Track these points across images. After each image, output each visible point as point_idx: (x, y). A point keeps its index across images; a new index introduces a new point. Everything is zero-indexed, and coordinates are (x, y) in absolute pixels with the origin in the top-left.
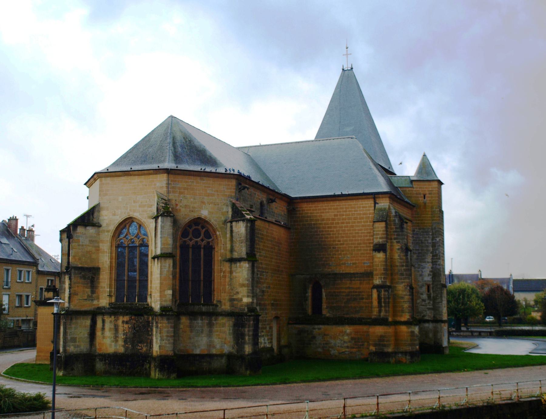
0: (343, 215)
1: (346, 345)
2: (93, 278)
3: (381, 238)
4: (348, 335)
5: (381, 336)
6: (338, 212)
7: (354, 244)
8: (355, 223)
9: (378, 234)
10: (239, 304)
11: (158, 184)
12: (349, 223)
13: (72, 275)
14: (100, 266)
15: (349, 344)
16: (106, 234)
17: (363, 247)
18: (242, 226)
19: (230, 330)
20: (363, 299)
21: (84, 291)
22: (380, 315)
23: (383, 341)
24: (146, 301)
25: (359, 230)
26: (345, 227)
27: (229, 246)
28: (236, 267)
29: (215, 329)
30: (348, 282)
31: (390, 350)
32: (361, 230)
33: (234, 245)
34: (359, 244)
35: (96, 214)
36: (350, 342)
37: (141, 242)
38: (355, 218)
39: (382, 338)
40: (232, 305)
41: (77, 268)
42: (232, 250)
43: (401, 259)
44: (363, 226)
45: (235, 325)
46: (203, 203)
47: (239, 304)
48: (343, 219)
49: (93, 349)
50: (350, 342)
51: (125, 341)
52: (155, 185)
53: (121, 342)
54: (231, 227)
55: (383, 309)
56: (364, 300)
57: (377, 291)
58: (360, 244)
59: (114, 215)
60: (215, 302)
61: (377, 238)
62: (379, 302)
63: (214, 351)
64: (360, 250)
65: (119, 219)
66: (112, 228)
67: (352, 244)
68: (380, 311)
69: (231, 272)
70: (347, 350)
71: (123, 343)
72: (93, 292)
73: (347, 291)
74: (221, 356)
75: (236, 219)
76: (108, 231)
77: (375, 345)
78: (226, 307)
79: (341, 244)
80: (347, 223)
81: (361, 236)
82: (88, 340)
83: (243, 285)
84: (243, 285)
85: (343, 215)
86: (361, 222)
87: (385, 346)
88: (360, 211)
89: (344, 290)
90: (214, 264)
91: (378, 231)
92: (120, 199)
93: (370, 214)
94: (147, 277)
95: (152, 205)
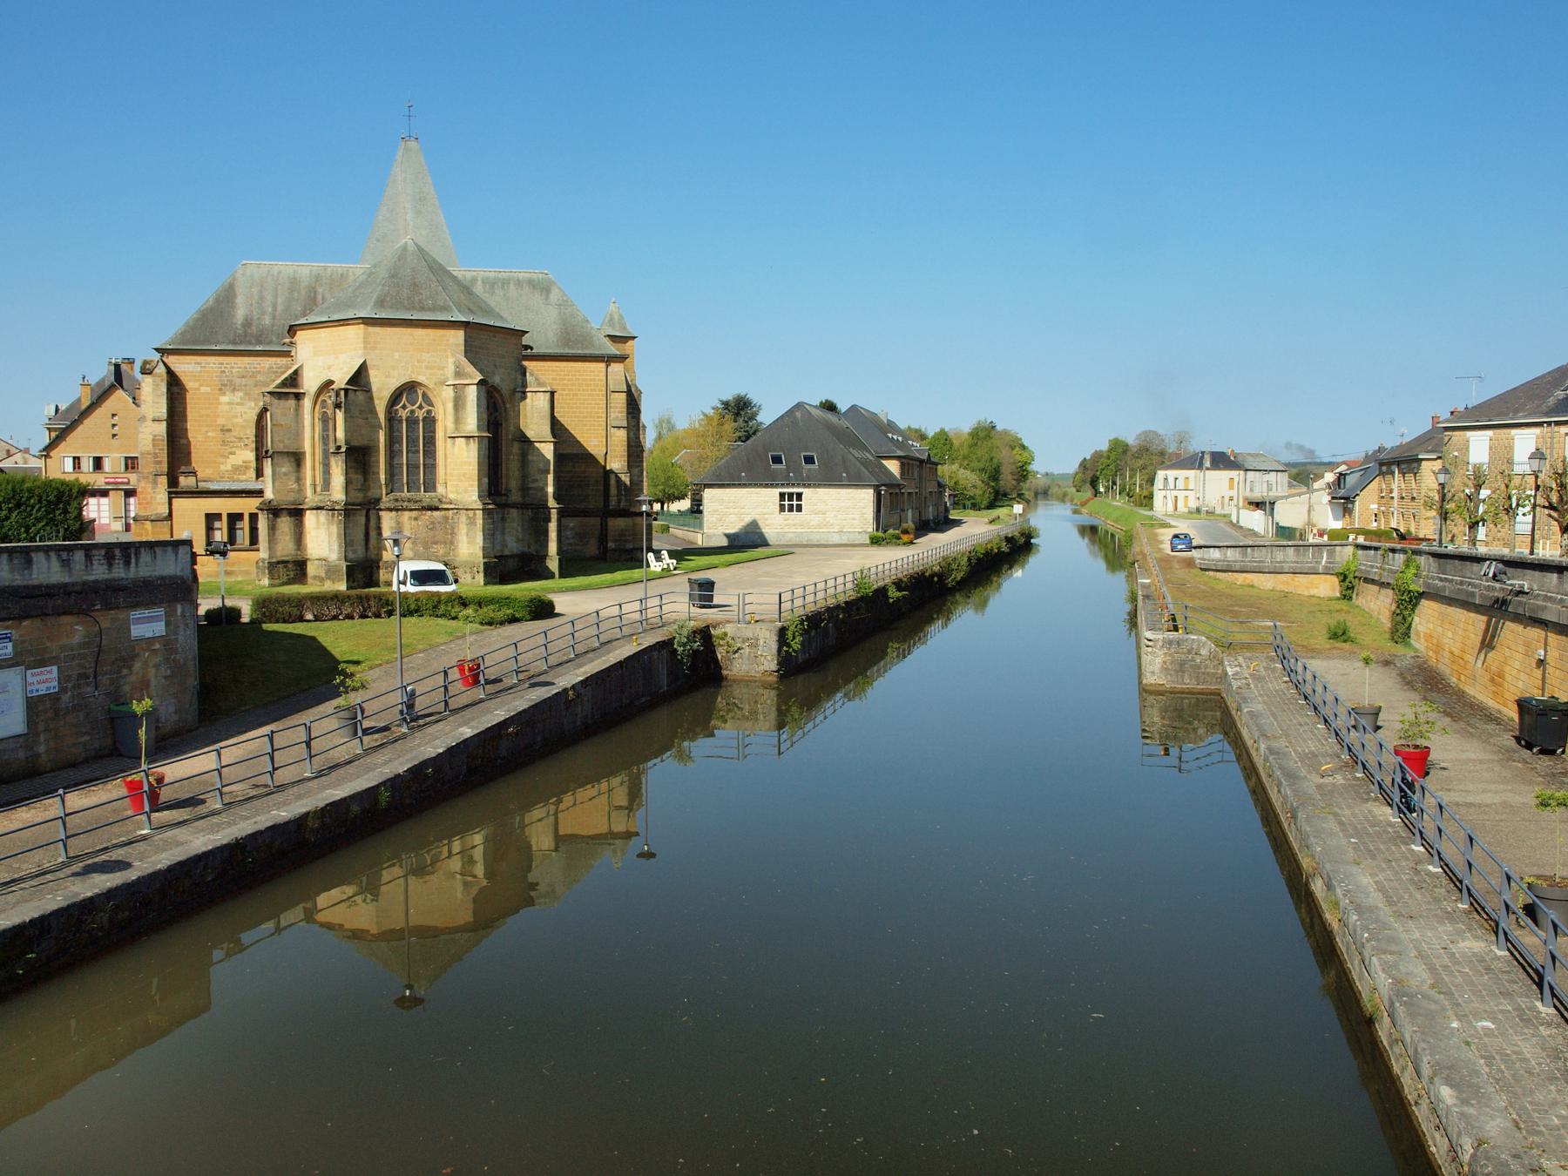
0: (564, 380)
1: (568, 541)
3: (619, 412)
4: (571, 529)
5: (622, 530)
6: (557, 375)
7: (578, 417)
8: (579, 390)
9: (617, 407)
10: (539, 494)
12: (572, 390)
15: (572, 541)
17: (589, 421)
18: (542, 398)
23: (625, 536)
24: (435, 491)
25: (584, 400)
26: (567, 395)
29: (507, 525)
31: (631, 547)
32: (587, 400)
34: (584, 417)
35: (363, 373)
36: (573, 538)
38: (580, 385)
40: (524, 496)
44: (589, 395)
45: (532, 519)
46: (495, 366)
47: (539, 494)
48: (564, 385)
49: (369, 554)
50: (573, 538)
59: (388, 376)
60: (503, 492)
61: (614, 412)
63: (507, 552)
64: (586, 425)
65: (395, 383)
67: (575, 417)
68: (619, 501)
72: (365, 480)
74: (513, 556)
77: (615, 541)
78: (515, 497)
80: (569, 390)
81: (587, 408)
82: (363, 543)
85: (564, 380)
86: (587, 390)
87: (626, 541)
88: (587, 375)
91: (617, 403)
92: (397, 355)
93: (599, 380)
94: (435, 460)
95: (444, 367)
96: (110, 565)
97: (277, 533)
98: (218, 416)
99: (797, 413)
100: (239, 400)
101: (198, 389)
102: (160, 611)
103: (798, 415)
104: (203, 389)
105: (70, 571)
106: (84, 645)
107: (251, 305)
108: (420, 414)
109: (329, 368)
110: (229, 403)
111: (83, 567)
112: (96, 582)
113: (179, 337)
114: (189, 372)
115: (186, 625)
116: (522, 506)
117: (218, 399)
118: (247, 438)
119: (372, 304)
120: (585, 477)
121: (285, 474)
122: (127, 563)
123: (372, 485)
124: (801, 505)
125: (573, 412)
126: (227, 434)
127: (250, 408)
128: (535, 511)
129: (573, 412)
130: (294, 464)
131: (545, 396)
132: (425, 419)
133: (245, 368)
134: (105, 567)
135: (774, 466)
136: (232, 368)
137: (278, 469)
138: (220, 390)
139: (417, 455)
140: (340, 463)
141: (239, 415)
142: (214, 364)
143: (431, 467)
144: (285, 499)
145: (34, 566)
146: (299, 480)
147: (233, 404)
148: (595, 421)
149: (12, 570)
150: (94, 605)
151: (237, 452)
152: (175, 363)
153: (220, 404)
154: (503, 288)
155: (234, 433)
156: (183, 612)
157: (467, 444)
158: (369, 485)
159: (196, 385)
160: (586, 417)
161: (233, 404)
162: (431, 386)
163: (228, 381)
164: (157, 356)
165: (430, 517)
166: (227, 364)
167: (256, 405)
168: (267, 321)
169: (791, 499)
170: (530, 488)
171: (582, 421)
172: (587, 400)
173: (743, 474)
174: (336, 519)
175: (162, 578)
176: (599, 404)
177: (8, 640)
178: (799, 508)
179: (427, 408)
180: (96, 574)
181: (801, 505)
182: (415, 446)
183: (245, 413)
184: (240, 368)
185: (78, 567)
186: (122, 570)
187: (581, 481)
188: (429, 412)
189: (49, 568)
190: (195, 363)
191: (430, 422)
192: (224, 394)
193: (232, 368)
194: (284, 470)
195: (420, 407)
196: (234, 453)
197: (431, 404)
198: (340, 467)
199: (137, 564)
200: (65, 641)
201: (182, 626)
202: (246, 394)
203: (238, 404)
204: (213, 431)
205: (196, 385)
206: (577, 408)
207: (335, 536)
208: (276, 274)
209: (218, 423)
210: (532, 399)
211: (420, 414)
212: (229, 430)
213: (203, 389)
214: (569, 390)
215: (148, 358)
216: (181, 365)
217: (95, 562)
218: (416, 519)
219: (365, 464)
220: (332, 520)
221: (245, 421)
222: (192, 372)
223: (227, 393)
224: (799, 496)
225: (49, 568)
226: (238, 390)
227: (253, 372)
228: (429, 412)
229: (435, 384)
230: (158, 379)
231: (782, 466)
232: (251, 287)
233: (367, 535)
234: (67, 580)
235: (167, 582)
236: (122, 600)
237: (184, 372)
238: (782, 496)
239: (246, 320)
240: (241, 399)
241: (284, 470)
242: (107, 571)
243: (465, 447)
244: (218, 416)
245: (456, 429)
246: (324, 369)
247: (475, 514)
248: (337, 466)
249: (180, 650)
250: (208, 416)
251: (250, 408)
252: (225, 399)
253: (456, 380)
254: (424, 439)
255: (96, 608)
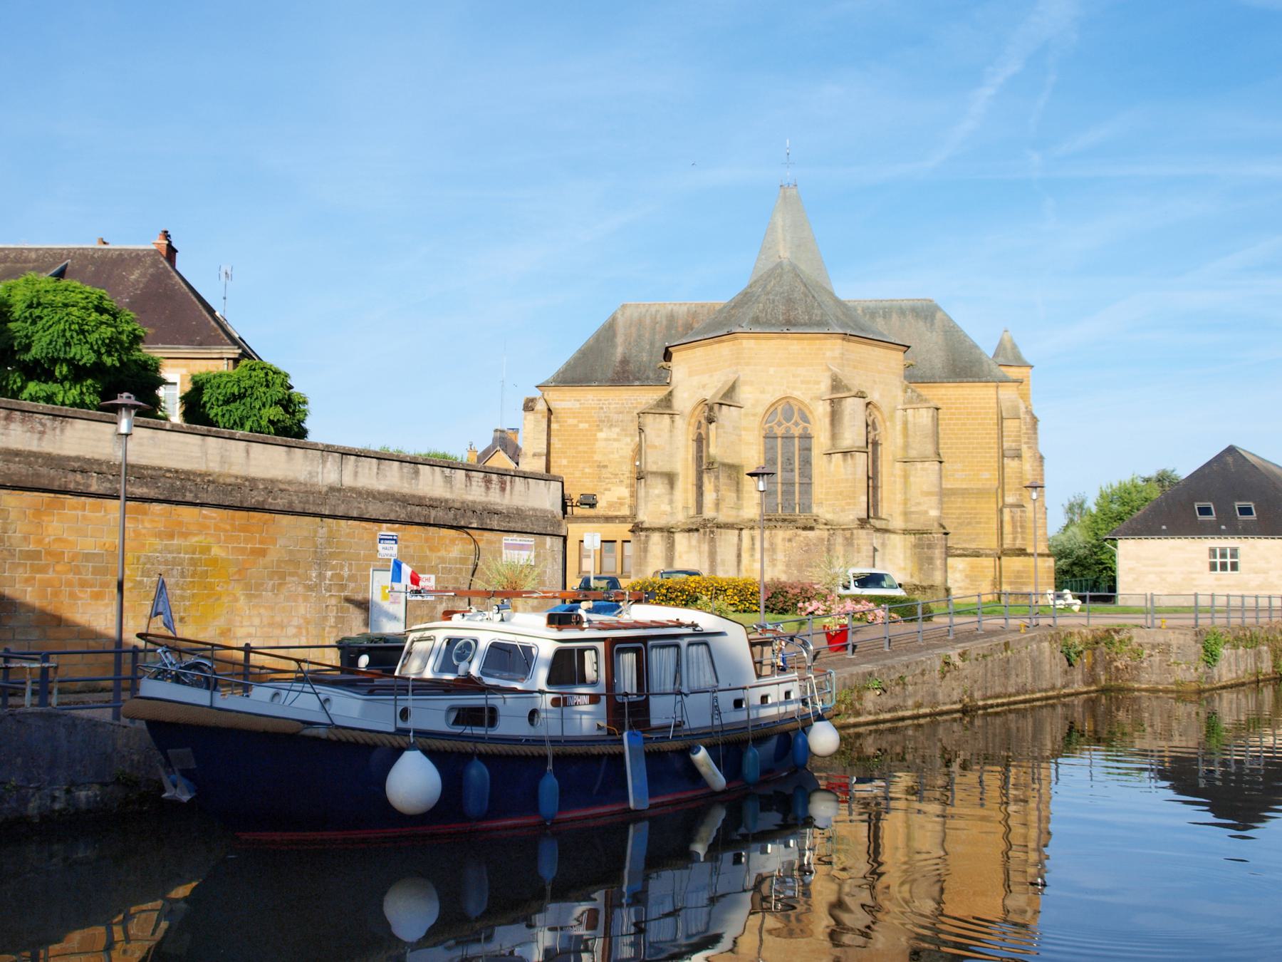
0: (951, 408)
1: (957, 585)
2: (738, 478)
3: (1014, 441)
5: (1018, 572)
8: (968, 419)
9: (1009, 436)
11: (829, 354)
13: (721, 474)
14: (744, 463)
15: (961, 584)
16: (752, 418)
17: (979, 453)
18: (925, 415)
19: (905, 552)
20: (980, 523)
21: (730, 496)
22: (1014, 544)
23: (1022, 577)
24: (811, 512)
26: (954, 424)
27: (899, 441)
28: (916, 469)
30: (960, 500)
32: (977, 429)
33: (911, 440)
34: (973, 448)
35: (737, 390)
36: (963, 581)
37: (801, 431)
39: (1019, 574)
40: (906, 521)
41: (724, 465)
42: (906, 447)
43: (1034, 470)
44: (979, 424)
45: (915, 546)
46: (874, 381)
50: (963, 581)
51: (788, 565)
52: (824, 354)
53: (780, 567)
54: (906, 416)
55: (1019, 536)
56: (982, 525)
57: (1011, 511)
58: (976, 448)
59: (762, 392)
61: (1008, 441)
62: (1014, 526)
65: (769, 398)
66: (761, 410)
68: (1014, 539)
69: (906, 477)
70: (960, 591)
71: (784, 568)
72: (738, 498)
73: (958, 511)
75: (914, 406)
76: (754, 415)
77: (1010, 583)
79: (948, 448)
80: (957, 419)
82: (736, 563)
83: (929, 494)
84: (929, 494)
85: (951, 408)
89: (954, 511)
90: (882, 466)
91: (1008, 431)
92: (772, 370)
93: (990, 408)
94: (810, 479)
96: (488, 488)
97: (650, 555)
98: (595, 452)
99: (1228, 458)
100: (615, 436)
101: (576, 426)
102: (530, 540)
103: (1229, 459)
104: (583, 426)
105: (451, 488)
106: (463, 560)
107: (630, 344)
108: (797, 431)
109: (704, 386)
110: (607, 440)
111: (464, 487)
112: (474, 502)
113: (561, 375)
114: (569, 409)
115: (554, 559)
116: (906, 532)
117: (595, 435)
118: (623, 474)
119: (747, 321)
120: (976, 514)
121: (658, 496)
122: (503, 489)
123: (745, 505)
124: (1236, 563)
125: (961, 444)
126: (604, 471)
127: (627, 444)
128: (917, 536)
129: (961, 444)
130: (668, 487)
131: (928, 412)
132: (800, 437)
133: (623, 404)
134: (483, 489)
135: (1201, 518)
136: (609, 404)
137: (651, 491)
138: (598, 426)
139: (793, 474)
140: (713, 480)
141: (615, 450)
142: (593, 400)
143: (807, 485)
144: (657, 521)
145: (421, 477)
146: (671, 502)
147: (609, 440)
148: (986, 453)
149: (402, 478)
150: (471, 523)
151: (612, 489)
152: (556, 400)
153: (597, 440)
154: (884, 317)
155: (610, 470)
156: (552, 546)
157: (845, 460)
158: (742, 505)
159: (574, 422)
160: (976, 448)
161: (609, 440)
162: (807, 401)
163: (606, 417)
164: (537, 394)
165: (804, 538)
166: (605, 400)
167: (632, 441)
168: (645, 357)
169: (1223, 555)
170: (912, 513)
171: (972, 453)
172: (977, 429)
173: (1164, 527)
174: (707, 537)
175: (534, 510)
176: (990, 434)
177: (394, 542)
178: (1234, 567)
179: (803, 424)
180: (474, 495)
181: (1236, 563)
182: (790, 464)
183: (622, 449)
184: (618, 404)
185: (458, 486)
186: (498, 495)
187: (971, 518)
188: (805, 428)
189: (433, 480)
190: (575, 400)
191: (806, 437)
192: (601, 430)
193: (609, 404)
194: (657, 492)
195: (796, 424)
196: (609, 490)
197: (807, 421)
198: (712, 484)
199: (511, 492)
200: (443, 553)
201: (550, 560)
202: (623, 430)
203: (615, 440)
204: (590, 467)
205: (574, 422)
206: (966, 438)
207: (706, 554)
208: (654, 313)
209: (596, 458)
210: (914, 417)
211: (797, 431)
212: (605, 467)
213: (583, 426)
214: (957, 419)
215: (531, 396)
216: (565, 400)
217: (474, 483)
218: (790, 540)
219: (738, 483)
220: (704, 538)
221: (621, 457)
222: (571, 409)
223: (604, 429)
224: (1234, 553)
225: (433, 480)
226: (616, 426)
227: (630, 408)
228: (805, 428)
229: (811, 399)
230: (539, 416)
231: (1213, 518)
232: (630, 327)
233: (739, 556)
234: (448, 495)
235: (538, 514)
236: (496, 522)
237: (564, 409)
238: (1213, 552)
239: (625, 357)
240: (618, 434)
241: (657, 492)
242: (484, 494)
243: (841, 463)
244: (595, 452)
245: (833, 445)
246: (699, 388)
247: (852, 534)
248: (710, 483)
249: (547, 583)
250: (585, 452)
251: (627, 444)
252: (601, 435)
253: (832, 393)
254: (799, 458)
255: (473, 526)
